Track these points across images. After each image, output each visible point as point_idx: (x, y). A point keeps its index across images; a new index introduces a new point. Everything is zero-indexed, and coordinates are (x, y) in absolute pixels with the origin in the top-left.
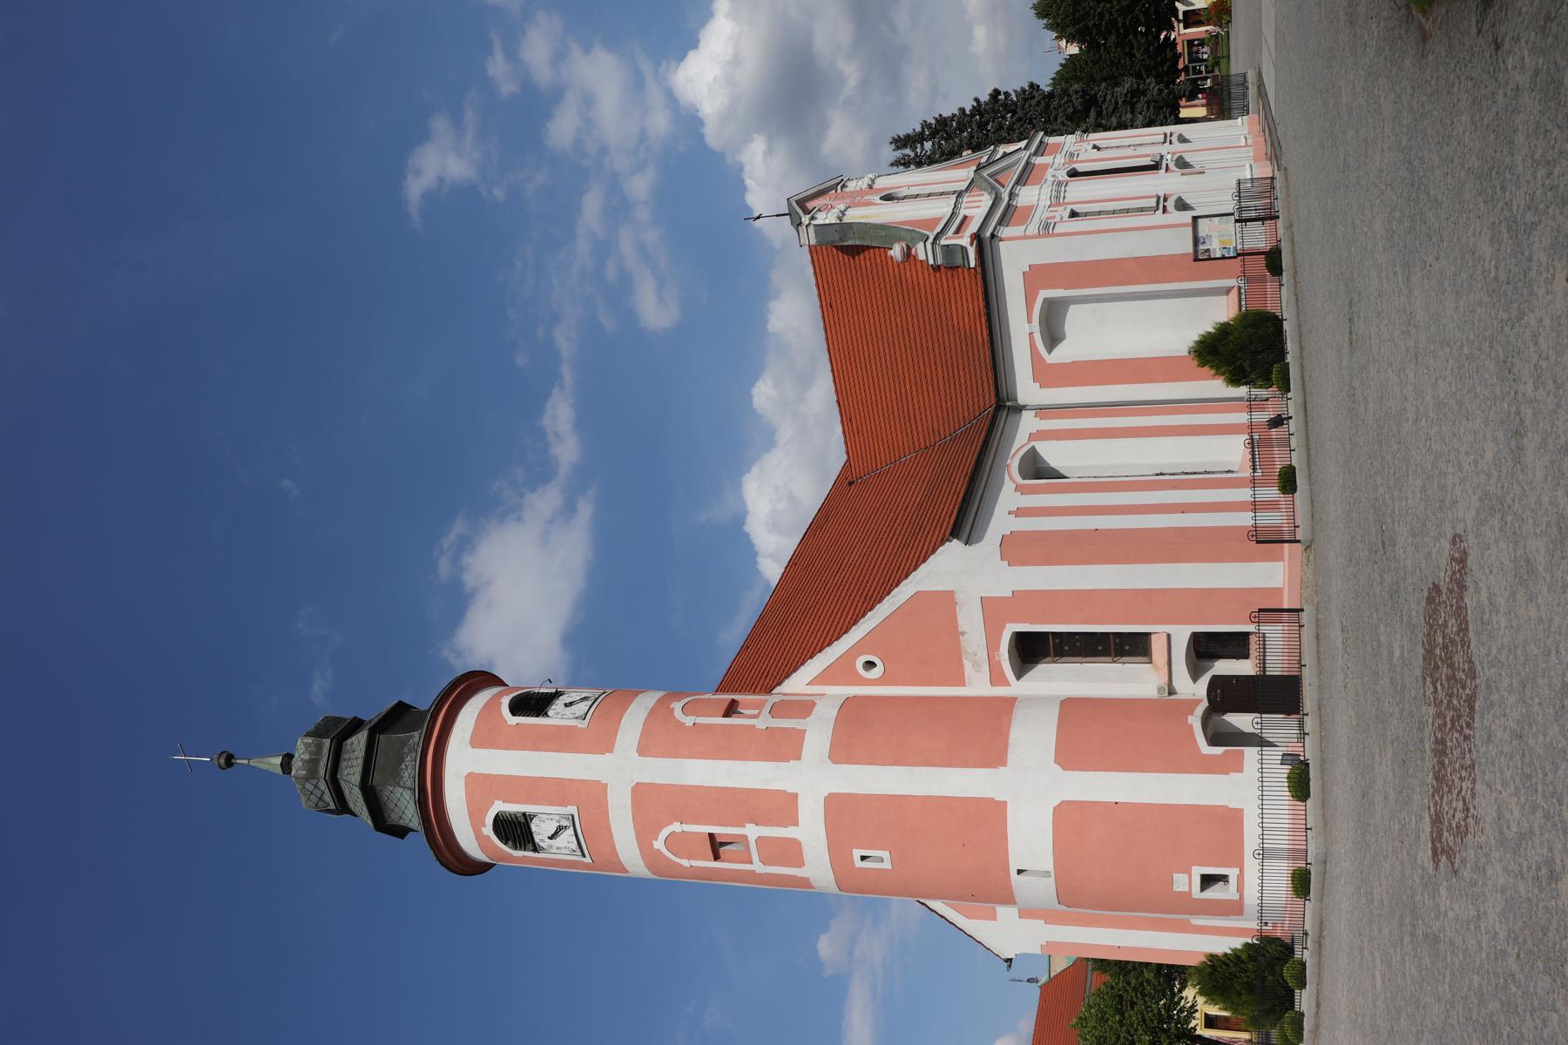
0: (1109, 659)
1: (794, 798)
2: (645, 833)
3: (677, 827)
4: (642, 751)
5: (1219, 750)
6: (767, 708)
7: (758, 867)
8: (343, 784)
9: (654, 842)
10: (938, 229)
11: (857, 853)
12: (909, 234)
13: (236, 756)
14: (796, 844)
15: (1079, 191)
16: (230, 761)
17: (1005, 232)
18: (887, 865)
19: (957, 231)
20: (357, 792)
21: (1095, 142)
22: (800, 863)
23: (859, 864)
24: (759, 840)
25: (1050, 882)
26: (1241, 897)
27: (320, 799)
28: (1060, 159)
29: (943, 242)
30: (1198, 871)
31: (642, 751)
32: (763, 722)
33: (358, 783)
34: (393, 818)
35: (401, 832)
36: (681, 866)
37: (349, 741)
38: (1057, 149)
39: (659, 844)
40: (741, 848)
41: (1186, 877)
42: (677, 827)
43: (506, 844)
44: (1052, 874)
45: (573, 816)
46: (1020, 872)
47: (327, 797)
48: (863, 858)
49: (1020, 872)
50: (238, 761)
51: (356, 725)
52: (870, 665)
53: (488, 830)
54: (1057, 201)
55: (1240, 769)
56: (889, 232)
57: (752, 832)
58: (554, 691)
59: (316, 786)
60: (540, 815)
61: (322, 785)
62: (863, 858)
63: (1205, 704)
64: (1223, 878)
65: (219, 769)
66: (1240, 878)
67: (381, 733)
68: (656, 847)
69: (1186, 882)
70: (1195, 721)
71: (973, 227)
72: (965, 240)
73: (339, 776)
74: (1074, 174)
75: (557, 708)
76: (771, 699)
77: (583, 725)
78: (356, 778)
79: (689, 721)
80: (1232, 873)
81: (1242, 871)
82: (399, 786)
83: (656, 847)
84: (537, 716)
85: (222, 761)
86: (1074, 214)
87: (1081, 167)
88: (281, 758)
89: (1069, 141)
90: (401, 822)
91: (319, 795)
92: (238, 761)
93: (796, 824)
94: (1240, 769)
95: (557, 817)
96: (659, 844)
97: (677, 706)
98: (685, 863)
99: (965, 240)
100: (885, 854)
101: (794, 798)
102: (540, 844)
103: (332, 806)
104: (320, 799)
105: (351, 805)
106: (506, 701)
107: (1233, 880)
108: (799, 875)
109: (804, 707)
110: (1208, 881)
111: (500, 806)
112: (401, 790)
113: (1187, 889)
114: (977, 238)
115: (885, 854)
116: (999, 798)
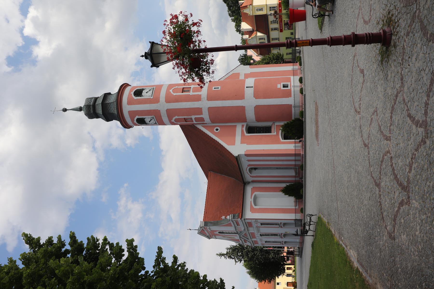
11: (214, 87)
18: (219, 89)
23: (213, 89)
25: (253, 88)
30: (282, 84)
41: (280, 85)
46: (247, 87)
49: (247, 87)
66: (290, 84)
69: (280, 86)
80: (289, 83)
81: (291, 83)
100: (219, 87)
110: (284, 86)
113: (280, 87)
115: (219, 87)
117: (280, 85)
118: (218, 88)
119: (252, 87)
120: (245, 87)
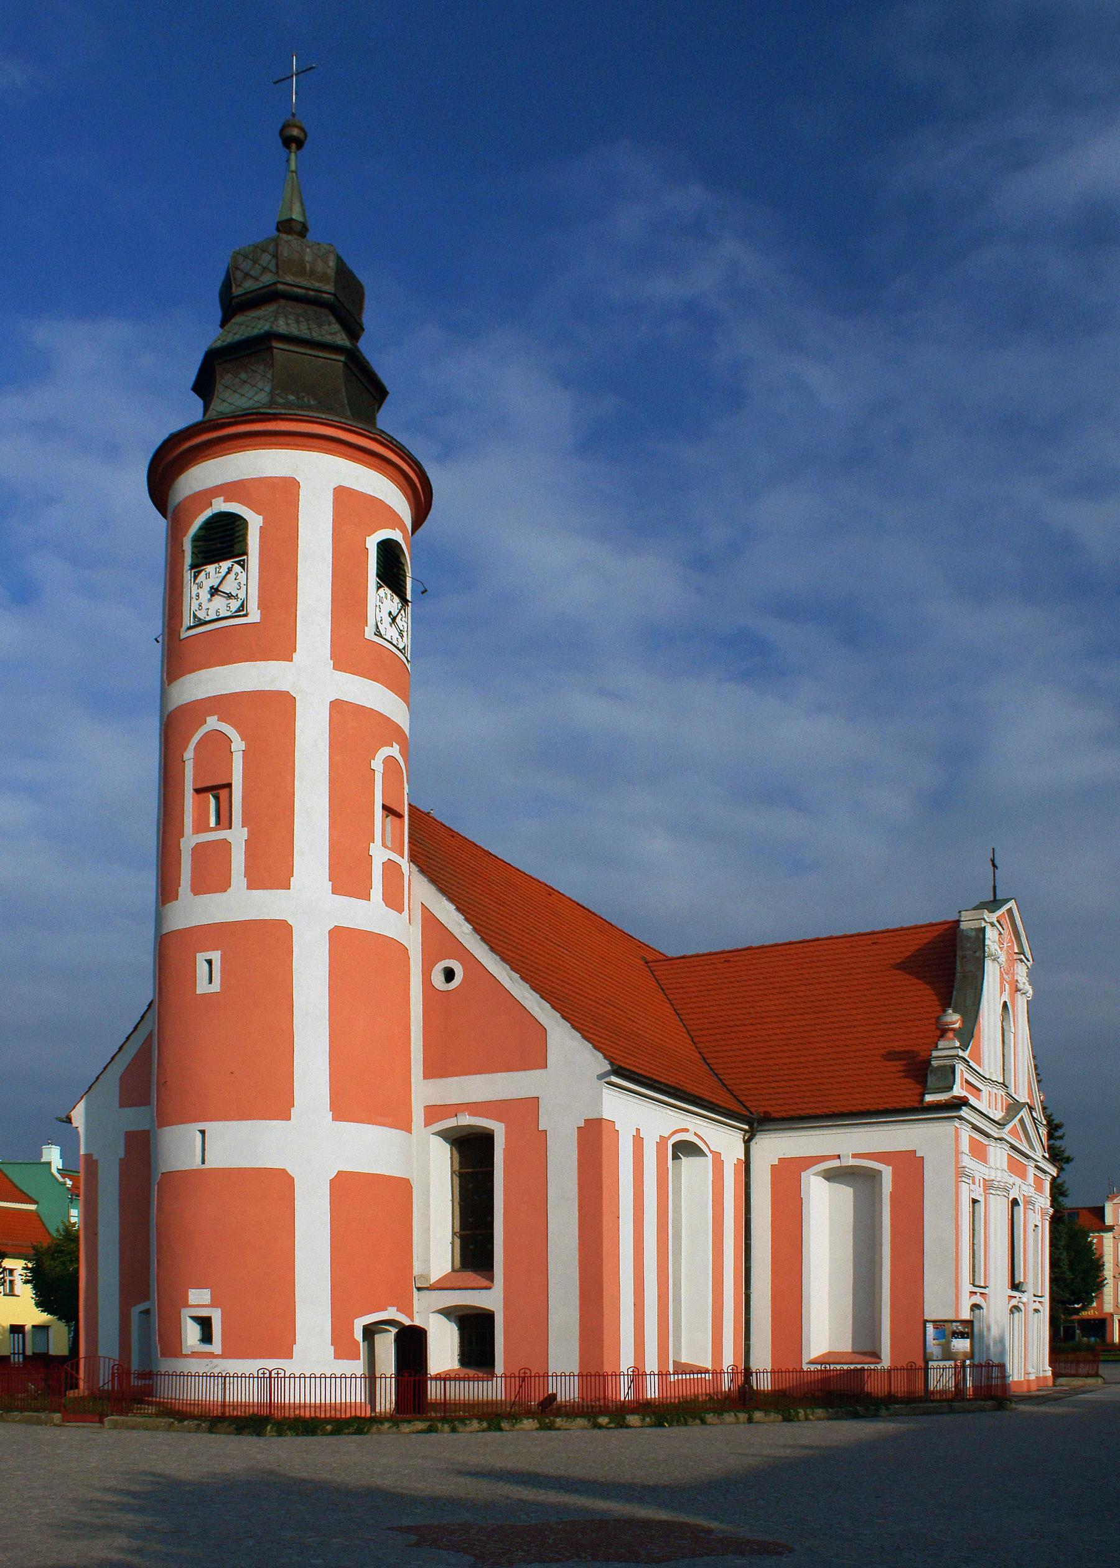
0: (457, 1229)
1: (284, 884)
2: (224, 705)
3: (238, 745)
4: (337, 706)
5: (358, 1335)
6: (395, 857)
7: (190, 840)
8: (272, 308)
9: (216, 717)
10: (972, 1063)
12: (968, 1034)
13: (299, 152)
14: (223, 884)
15: (998, 1209)
16: (291, 141)
17: (966, 1133)
19: (967, 1082)
20: (262, 327)
21: (1040, 1228)
22: (198, 888)
24: (226, 845)
25: (196, 1163)
26: (186, 1356)
27: (247, 275)
28: (1030, 1191)
29: (960, 1067)
31: (337, 706)
32: (379, 854)
33: (275, 328)
34: (224, 379)
35: (204, 386)
36: (185, 748)
37: (332, 319)
38: (1039, 1188)
39: (213, 723)
40: (212, 823)
41: (208, 1302)
42: (238, 745)
43: (201, 528)
44: (204, 1167)
45: (245, 615)
46: (203, 1132)
47: (249, 285)
48: (210, 962)
50: (293, 156)
51: (354, 329)
52: (449, 975)
53: (221, 505)
54: (988, 1185)
55: (338, 1356)
56: (972, 1015)
57: (237, 836)
58: (409, 597)
59: (265, 269)
60: (244, 574)
61: (267, 279)
62: (210, 962)
63: (407, 1322)
64: (207, 1338)
65: (280, 126)
66: (211, 1355)
67: (345, 363)
68: (208, 719)
70: (391, 1313)
71: (973, 1101)
72: (958, 1090)
73: (282, 302)
74: (1015, 1203)
75: (392, 603)
76: (404, 863)
77: (369, 633)
78: (282, 326)
79: (377, 764)
80: (216, 1346)
82: (273, 388)
83: (208, 719)
84: (378, 575)
85: (295, 132)
86: (975, 1201)
87: (1020, 1210)
88: (302, 220)
89: (1044, 1201)
90: (219, 388)
91: (252, 273)
92: (293, 156)
93: (251, 886)
94: (338, 1356)
95: (242, 595)
96: (213, 723)
97: (394, 751)
98: (189, 754)
99: (958, 1090)
101: (284, 884)
102: (203, 573)
103: (236, 291)
104: (247, 275)
105: (238, 319)
106: (396, 535)
107: (206, 1348)
108: (180, 889)
109: (394, 899)
110: (205, 1323)
111: (255, 522)
112: (267, 389)
114: (963, 1102)
115: (216, 987)
116: (294, 1112)
117: (208, 1302)
118: (211, 982)
119: (203, 1162)
120: (202, 1125)
